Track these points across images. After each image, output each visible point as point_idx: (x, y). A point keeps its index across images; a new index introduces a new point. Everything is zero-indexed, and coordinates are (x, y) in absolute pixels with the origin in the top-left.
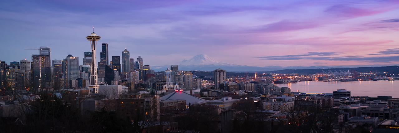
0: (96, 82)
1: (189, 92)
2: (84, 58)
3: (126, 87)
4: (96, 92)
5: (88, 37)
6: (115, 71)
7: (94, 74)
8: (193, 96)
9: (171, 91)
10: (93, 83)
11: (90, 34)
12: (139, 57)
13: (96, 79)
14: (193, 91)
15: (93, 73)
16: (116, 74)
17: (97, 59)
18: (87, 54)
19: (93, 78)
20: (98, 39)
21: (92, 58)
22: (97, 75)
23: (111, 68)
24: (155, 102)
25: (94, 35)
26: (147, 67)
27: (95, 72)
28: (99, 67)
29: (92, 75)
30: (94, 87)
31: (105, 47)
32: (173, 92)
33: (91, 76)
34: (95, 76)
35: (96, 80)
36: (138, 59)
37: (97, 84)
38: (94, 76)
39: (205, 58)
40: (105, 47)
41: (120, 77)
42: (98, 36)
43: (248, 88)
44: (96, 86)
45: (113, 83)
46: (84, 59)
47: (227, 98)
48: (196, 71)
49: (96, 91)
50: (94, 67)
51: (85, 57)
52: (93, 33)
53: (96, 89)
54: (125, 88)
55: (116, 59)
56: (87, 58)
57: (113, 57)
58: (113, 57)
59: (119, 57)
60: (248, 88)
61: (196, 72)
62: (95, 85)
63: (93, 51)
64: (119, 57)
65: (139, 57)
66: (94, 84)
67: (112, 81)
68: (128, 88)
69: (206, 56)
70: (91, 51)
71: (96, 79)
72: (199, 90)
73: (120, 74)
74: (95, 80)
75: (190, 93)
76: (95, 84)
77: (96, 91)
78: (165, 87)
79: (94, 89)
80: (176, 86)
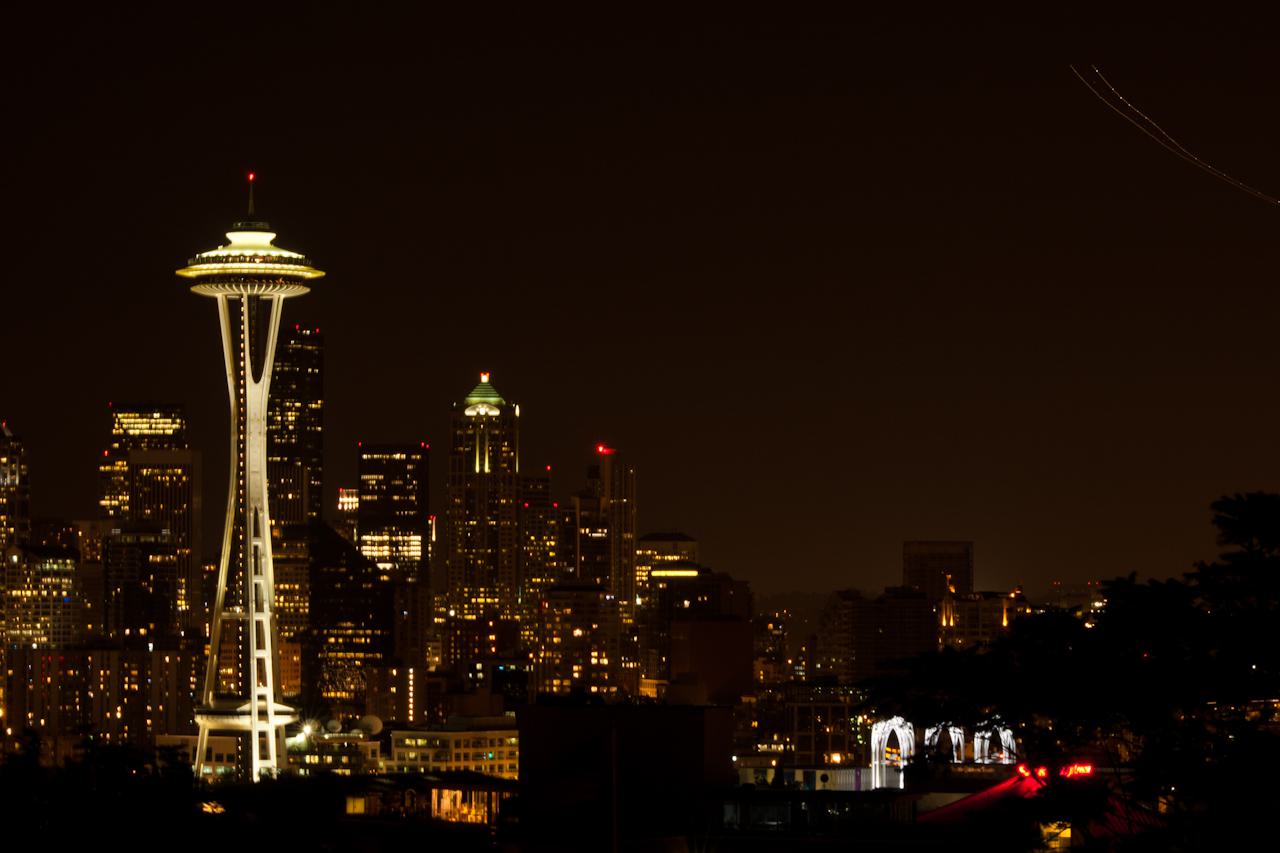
0: (262, 678)
4: (258, 766)
13: (260, 645)
19: (237, 642)
30: (242, 722)
35: (266, 654)
37: (268, 691)
38: (245, 624)
44: (263, 714)
49: (264, 756)
53: (263, 735)
62: (255, 705)
66: (246, 696)
71: (260, 645)
74: (256, 654)
76: (257, 690)
77: (264, 756)
78: (893, 741)
79: (246, 735)
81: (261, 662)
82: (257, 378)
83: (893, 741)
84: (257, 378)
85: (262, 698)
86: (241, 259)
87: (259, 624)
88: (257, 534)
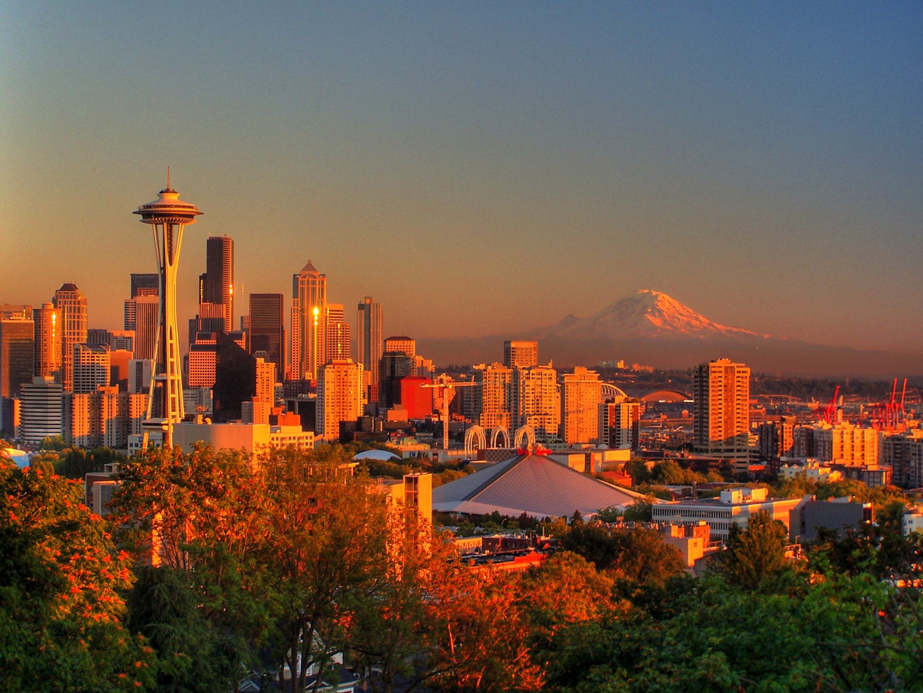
1: (577, 462)
2: (128, 296)
3: (304, 430)
5: (144, 207)
6: (260, 361)
7: (164, 370)
8: (598, 477)
9: (500, 456)
10: (160, 410)
11: (150, 198)
12: (366, 298)
13: (173, 392)
14: (597, 457)
15: (162, 367)
16: (265, 369)
17: (179, 306)
18: (141, 283)
20: (191, 216)
21: (158, 300)
22: (178, 377)
23: (242, 343)
24: (413, 499)
25: (172, 198)
26: (400, 343)
27: (169, 360)
28: (192, 339)
29: (157, 373)
30: (165, 428)
31: (217, 250)
32: (503, 460)
33: (157, 381)
34: (170, 377)
36: (361, 307)
37: (177, 413)
38: (165, 382)
39: (660, 311)
40: (217, 250)
41: (278, 384)
42: (191, 207)
43: (847, 446)
45: (251, 409)
46: (127, 304)
47: (746, 491)
48: (620, 365)
50: (169, 342)
51: (134, 293)
52: (167, 191)
54: (299, 438)
55: (266, 305)
56: (141, 299)
57: (253, 296)
58: (253, 296)
59: (279, 297)
60: (847, 446)
61: (619, 370)
63: (163, 269)
64: (279, 297)
65: (366, 298)
66: (165, 415)
67: (246, 403)
68: (312, 434)
69: (666, 302)
70: (156, 270)
72: (623, 455)
73: (280, 377)
74: (170, 396)
76: (171, 413)
78: (476, 437)
80: (525, 433)
81: (173, 399)
82: (171, 265)
83: (476, 437)
84: (171, 265)
85: (173, 417)
86: (165, 206)
87: (173, 381)
88: (171, 338)
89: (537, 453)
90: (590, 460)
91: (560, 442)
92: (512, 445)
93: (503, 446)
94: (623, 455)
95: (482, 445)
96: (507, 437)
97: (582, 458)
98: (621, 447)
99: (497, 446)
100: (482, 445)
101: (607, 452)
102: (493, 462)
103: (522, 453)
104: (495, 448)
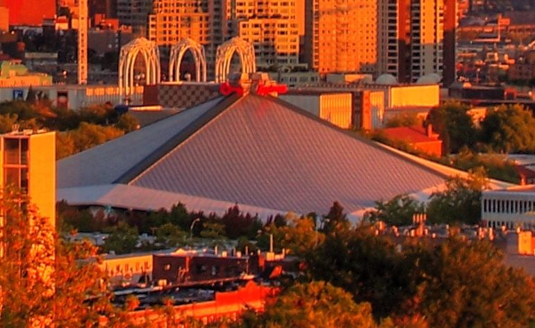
1: (336, 108)
8: (377, 138)
14: (376, 99)
32: (194, 105)
72: (424, 95)
75: (344, 120)
78: (140, 61)
80: (236, 53)
83: (140, 61)
89: (260, 91)
90: (361, 105)
91: (304, 70)
92: (211, 76)
93: (194, 78)
94: (424, 95)
95: (152, 75)
96: (200, 61)
97: (346, 101)
98: (420, 80)
99: (182, 78)
100: (152, 75)
101: (393, 89)
102: (174, 109)
103: (231, 92)
104: (178, 82)
